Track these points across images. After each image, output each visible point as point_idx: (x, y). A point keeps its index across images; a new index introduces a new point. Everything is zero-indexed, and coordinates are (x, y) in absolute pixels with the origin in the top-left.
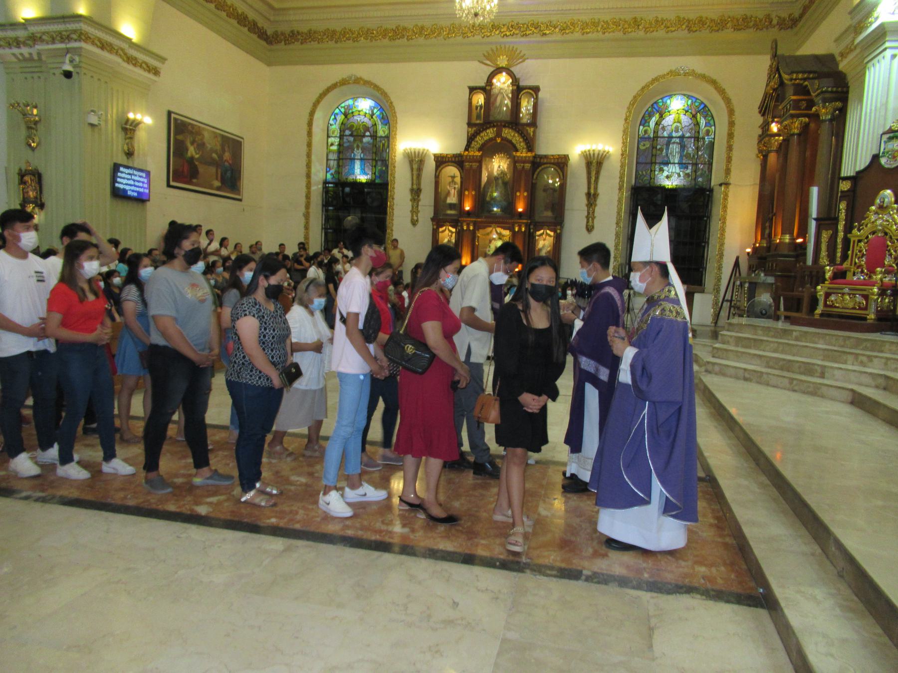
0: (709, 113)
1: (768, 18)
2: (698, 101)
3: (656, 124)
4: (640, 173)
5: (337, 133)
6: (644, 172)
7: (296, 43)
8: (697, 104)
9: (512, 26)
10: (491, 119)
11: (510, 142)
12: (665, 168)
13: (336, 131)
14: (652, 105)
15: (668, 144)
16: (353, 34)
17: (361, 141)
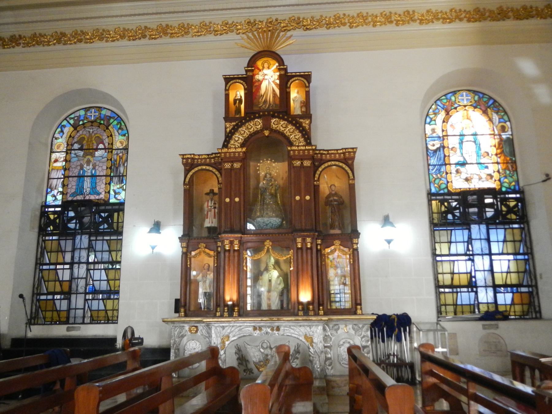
0: (501, 109)
2: (485, 96)
3: (444, 122)
4: (434, 176)
5: (63, 148)
6: (439, 175)
7: (16, 47)
8: (485, 100)
9: (270, 22)
10: (255, 109)
11: (282, 134)
12: (462, 169)
13: (63, 145)
14: (435, 102)
15: (461, 143)
16: (86, 35)
17: (93, 155)
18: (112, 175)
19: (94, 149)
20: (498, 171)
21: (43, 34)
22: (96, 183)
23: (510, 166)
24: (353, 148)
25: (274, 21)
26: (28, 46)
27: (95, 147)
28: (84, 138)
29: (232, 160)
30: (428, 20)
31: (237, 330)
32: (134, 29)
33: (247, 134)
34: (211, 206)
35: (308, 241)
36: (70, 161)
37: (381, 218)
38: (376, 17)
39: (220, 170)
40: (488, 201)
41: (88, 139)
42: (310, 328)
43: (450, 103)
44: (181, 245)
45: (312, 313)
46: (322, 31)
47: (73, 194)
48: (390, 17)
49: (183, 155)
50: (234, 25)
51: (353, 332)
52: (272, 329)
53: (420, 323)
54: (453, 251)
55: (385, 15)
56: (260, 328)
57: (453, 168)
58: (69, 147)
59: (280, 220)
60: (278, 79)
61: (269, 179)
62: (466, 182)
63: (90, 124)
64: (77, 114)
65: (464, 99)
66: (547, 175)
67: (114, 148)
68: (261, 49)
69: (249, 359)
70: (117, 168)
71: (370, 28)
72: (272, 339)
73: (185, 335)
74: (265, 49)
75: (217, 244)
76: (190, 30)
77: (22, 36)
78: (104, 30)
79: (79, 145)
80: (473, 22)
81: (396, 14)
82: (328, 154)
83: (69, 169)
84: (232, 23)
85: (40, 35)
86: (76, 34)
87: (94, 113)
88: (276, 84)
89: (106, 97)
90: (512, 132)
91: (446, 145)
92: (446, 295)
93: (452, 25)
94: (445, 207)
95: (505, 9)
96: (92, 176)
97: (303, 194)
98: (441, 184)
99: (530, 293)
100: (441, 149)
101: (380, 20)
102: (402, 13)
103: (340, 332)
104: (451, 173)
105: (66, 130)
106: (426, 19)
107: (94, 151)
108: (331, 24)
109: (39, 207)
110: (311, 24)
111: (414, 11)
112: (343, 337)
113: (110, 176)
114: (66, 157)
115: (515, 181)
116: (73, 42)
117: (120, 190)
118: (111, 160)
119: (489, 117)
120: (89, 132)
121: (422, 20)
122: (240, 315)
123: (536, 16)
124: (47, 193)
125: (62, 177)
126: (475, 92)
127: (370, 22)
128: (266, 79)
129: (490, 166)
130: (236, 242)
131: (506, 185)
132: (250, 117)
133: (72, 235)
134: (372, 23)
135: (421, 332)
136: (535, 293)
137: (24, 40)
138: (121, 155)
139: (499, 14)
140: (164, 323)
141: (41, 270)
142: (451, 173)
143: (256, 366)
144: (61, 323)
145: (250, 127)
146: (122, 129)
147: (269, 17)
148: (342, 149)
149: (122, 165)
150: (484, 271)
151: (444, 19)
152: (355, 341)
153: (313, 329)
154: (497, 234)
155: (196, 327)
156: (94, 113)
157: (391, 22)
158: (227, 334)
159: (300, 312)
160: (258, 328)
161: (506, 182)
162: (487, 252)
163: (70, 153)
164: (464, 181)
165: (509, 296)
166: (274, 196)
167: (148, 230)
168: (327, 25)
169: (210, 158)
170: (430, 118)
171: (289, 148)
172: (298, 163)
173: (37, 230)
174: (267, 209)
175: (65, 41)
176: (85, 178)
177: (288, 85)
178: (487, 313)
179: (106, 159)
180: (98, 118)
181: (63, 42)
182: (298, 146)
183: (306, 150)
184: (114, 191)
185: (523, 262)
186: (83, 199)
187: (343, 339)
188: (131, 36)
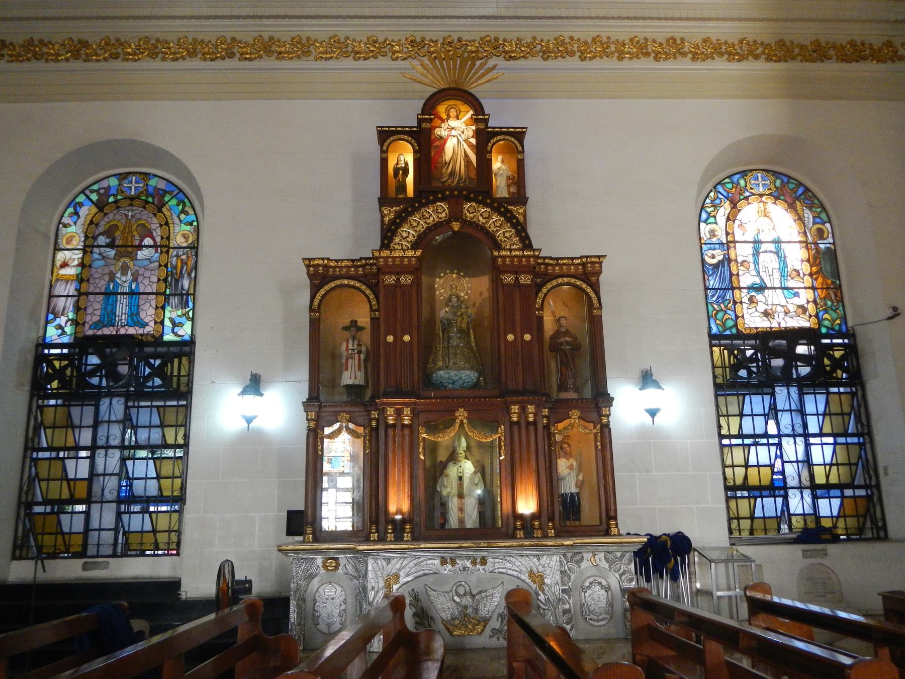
0: (816, 202)
1: (888, 44)
2: (792, 181)
3: (728, 219)
4: (716, 306)
5: (79, 242)
6: (722, 306)
8: (791, 186)
9: (450, 44)
10: (435, 184)
11: (483, 229)
12: (759, 297)
13: (77, 238)
14: (715, 187)
15: (756, 254)
17: (134, 258)
18: (168, 292)
19: (135, 246)
20: (815, 302)
21: (46, 42)
22: (138, 306)
23: (832, 293)
24: (599, 257)
25: (456, 41)
26: (18, 60)
27: (137, 243)
28: (116, 227)
29: (399, 269)
30: (706, 55)
31: (412, 564)
32: (213, 42)
33: (422, 226)
34: (353, 350)
35: (530, 411)
36: (90, 266)
37: (637, 375)
38: (624, 44)
39: (374, 288)
40: (801, 349)
41: (124, 229)
42: (539, 560)
43: (738, 189)
44: (307, 415)
45: (538, 533)
46: (536, 62)
47: (99, 325)
48: (646, 46)
49: (310, 260)
50: (387, 44)
51: (606, 566)
52: (474, 563)
53: (704, 548)
54: (747, 429)
55: (638, 42)
56: (453, 562)
57: (744, 295)
58: (89, 242)
59: (476, 374)
60: (473, 137)
61: (456, 305)
62: (765, 318)
63: (128, 202)
64: (104, 184)
65: (760, 184)
66: (895, 309)
67: (171, 245)
68: (444, 86)
69: (435, 615)
70: (177, 281)
71: (613, 63)
72: (473, 579)
73: (316, 575)
74: (452, 86)
75: (369, 415)
76: (312, 48)
77: (8, 43)
78: (158, 40)
79: (108, 238)
80: (775, 61)
81: (654, 41)
82: (557, 264)
83: (88, 281)
84: (385, 41)
85: (41, 42)
86: (107, 44)
87: (136, 183)
88: (470, 145)
89: (160, 156)
90: (834, 240)
91: (732, 256)
92: (739, 501)
93: (743, 65)
94: (735, 357)
95: (824, 45)
96: (132, 293)
97: (518, 330)
98: (727, 319)
99: (869, 498)
100: (726, 263)
101: (630, 50)
102: (664, 42)
103: (584, 565)
104: (741, 303)
105: (83, 211)
106: (703, 53)
107: (135, 249)
108: (551, 53)
109: (31, 346)
110: (518, 50)
111: (682, 40)
112: (590, 574)
113: (164, 294)
114: (83, 258)
115: (841, 319)
116: (101, 58)
117: (183, 319)
118: (166, 266)
119: (798, 214)
120: (127, 216)
121: (697, 53)
122: (415, 539)
123: (871, 58)
124: (47, 322)
125: (76, 293)
126: (776, 174)
127: (613, 53)
128: (454, 136)
129: (802, 292)
130: (407, 411)
131: (826, 323)
132: (427, 199)
133: (94, 397)
134: (616, 55)
135: (713, 564)
136: (875, 499)
137: (11, 50)
138: (184, 257)
139: (814, 51)
140: (280, 554)
141: (36, 461)
142: (741, 303)
143: (446, 627)
144: (76, 555)
145: (427, 216)
146: (187, 214)
147: (447, 34)
148: (581, 257)
149: (185, 276)
150: (797, 462)
151: (730, 54)
152: (609, 580)
153: (545, 560)
154: (814, 403)
155: (336, 559)
156: (136, 183)
157: (647, 54)
158: (393, 571)
159: (518, 532)
160: (449, 560)
161: (826, 319)
162: (800, 431)
163: (91, 252)
164: (762, 315)
165: (836, 502)
166: (464, 333)
167: (240, 390)
168: (544, 53)
169: (357, 267)
170: (706, 212)
171: (496, 253)
172: (509, 279)
173: (27, 388)
174: (455, 354)
175: (87, 55)
176: (119, 296)
177: (489, 148)
178: (806, 530)
179: (157, 264)
180: (142, 192)
181: (83, 57)
182: (510, 250)
183: (524, 256)
184: (172, 320)
185: (857, 448)
186: (114, 333)
187: (589, 577)
188: (208, 54)
